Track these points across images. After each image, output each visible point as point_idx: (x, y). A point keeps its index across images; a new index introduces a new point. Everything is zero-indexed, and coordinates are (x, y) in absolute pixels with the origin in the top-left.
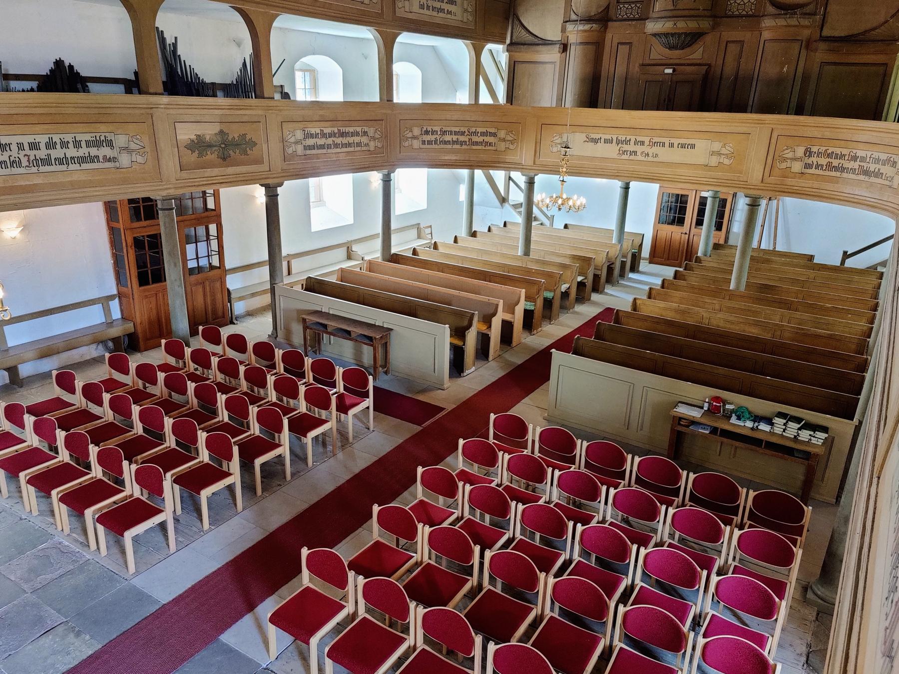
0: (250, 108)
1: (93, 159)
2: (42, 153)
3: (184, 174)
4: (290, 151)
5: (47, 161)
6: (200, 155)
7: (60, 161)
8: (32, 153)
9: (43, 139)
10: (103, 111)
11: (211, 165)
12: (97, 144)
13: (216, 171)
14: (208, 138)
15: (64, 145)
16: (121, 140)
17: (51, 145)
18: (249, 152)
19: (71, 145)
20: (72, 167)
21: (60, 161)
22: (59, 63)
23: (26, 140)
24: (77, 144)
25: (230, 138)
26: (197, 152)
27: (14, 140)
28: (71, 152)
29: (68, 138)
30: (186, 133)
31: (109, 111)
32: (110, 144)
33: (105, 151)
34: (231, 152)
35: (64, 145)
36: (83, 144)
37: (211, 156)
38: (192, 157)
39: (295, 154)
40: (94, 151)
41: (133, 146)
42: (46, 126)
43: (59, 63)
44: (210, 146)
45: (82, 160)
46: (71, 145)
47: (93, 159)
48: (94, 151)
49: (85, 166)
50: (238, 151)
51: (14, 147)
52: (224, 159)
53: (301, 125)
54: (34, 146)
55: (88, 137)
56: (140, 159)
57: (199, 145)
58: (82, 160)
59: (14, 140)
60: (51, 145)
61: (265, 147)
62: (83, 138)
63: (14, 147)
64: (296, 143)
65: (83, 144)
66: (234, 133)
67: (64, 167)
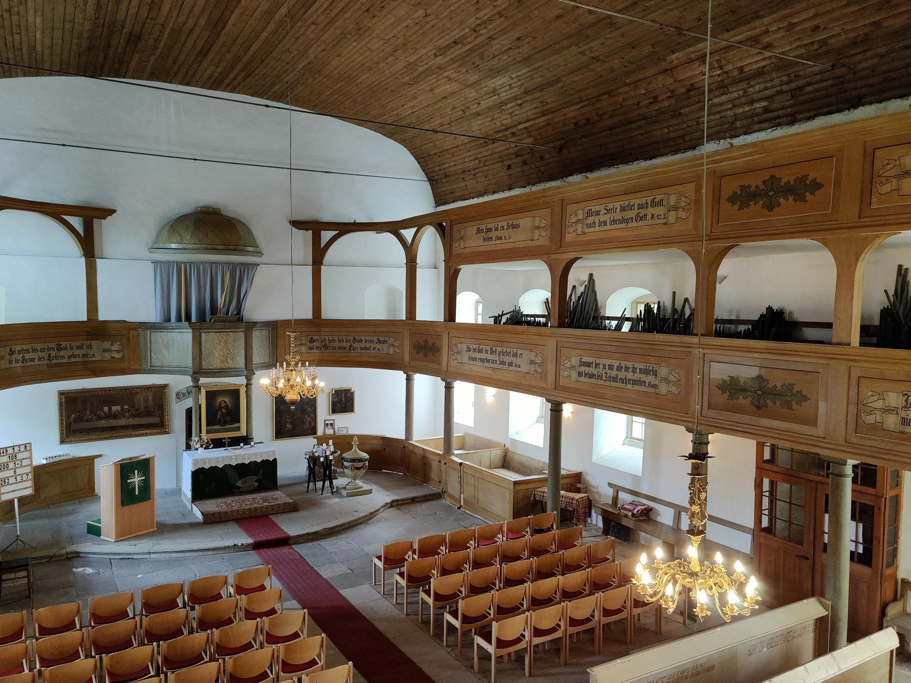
0: (795, 353)
1: (641, 383)
2: (614, 373)
3: (711, 413)
4: (871, 419)
5: (615, 379)
6: (731, 397)
7: (623, 381)
8: (609, 372)
9: (616, 363)
10: (654, 347)
11: (741, 410)
12: (646, 372)
13: (746, 418)
14: (742, 382)
15: (627, 369)
16: (663, 371)
17: (619, 368)
18: (795, 406)
19: (630, 370)
20: (629, 386)
21: (623, 381)
22: (770, 309)
23: (608, 362)
24: (634, 370)
25: (770, 385)
26: (728, 393)
27: (601, 361)
28: (630, 376)
29: (630, 365)
30: (720, 371)
31: (659, 347)
32: (655, 374)
33: (650, 379)
34: (769, 401)
35: (627, 369)
36: (638, 370)
37: (743, 401)
38: (722, 398)
39: (877, 428)
40: (643, 377)
41: (672, 378)
42: (619, 355)
43: (770, 309)
44: (743, 390)
45: (635, 382)
46: (630, 370)
47: (641, 383)
48: (643, 377)
49: (636, 387)
50: (778, 403)
51: (601, 366)
52: (759, 407)
53: (902, 387)
54: (611, 367)
55: (641, 366)
56: (674, 390)
57: (732, 387)
58: (635, 382)
59: (601, 361)
60: (619, 368)
61: (822, 405)
62: (639, 366)
63: (601, 366)
64: (887, 410)
65: (638, 370)
66: (778, 381)
67: (623, 385)
